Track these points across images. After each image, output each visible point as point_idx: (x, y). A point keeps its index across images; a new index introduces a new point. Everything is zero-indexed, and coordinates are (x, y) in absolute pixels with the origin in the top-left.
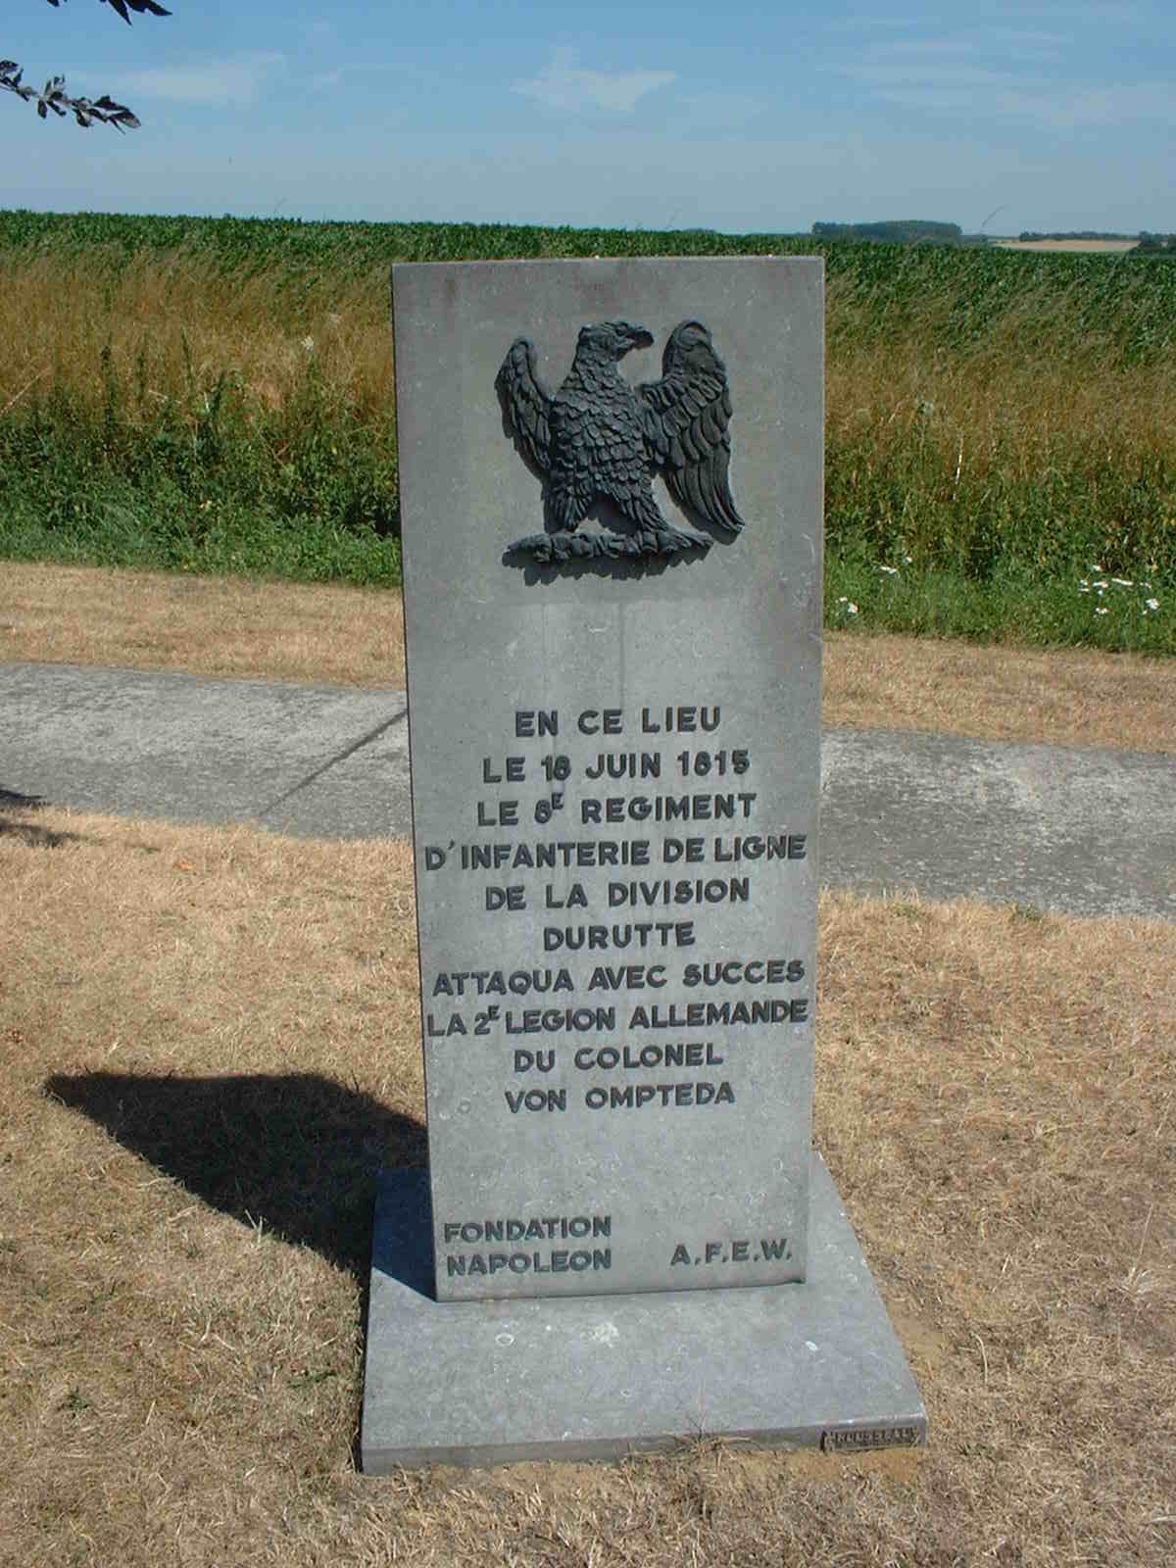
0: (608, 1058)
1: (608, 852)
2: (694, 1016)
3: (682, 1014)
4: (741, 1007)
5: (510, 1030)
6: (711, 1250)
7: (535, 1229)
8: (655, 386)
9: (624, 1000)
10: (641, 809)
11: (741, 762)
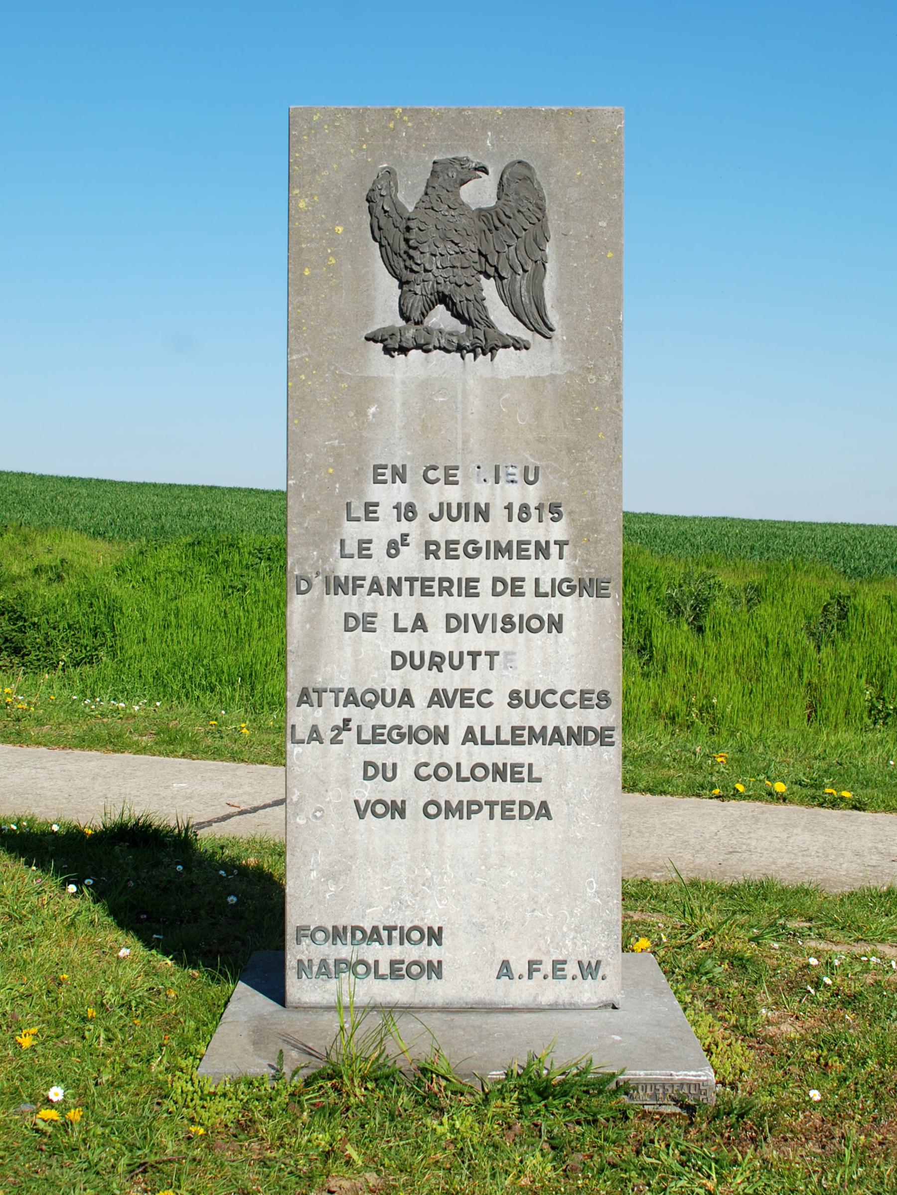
0: (443, 772)
1: (446, 586)
2: (516, 737)
3: (506, 735)
4: (557, 730)
5: (360, 741)
6: (533, 967)
7: (374, 935)
8: (488, 210)
9: (458, 720)
10: (473, 549)
11: (555, 510)
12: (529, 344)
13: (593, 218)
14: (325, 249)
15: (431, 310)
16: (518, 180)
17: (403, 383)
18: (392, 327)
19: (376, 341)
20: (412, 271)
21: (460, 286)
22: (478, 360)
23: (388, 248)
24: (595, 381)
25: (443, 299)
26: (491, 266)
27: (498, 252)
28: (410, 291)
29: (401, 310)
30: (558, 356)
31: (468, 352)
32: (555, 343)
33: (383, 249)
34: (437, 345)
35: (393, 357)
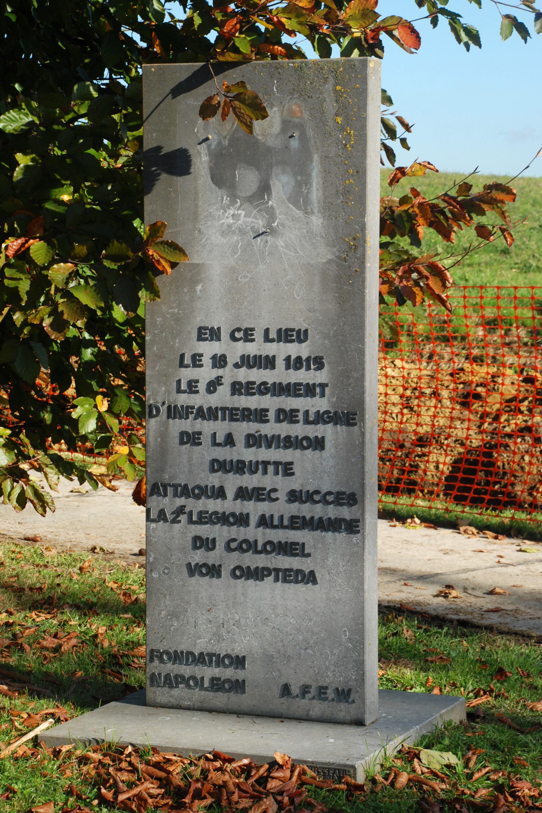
9: (254, 509)
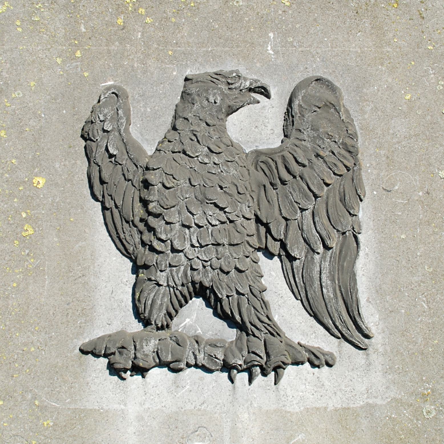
8: (270, 154)
12: (334, 360)
13: (430, 165)
14: (17, 212)
15: (181, 306)
16: (314, 107)
17: (140, 418)
18: (121, 333)
19: (97, 356)
20: (152, 249)
21: (227, 273)
22: (255, 382)
23: (115, 211)
24: (434, 413)
25: (201, 291)
26: (275, 240)
27: (286, 219)
28: (150, 280)
29: (135, 308)
30: (377, 378)
31: (239, 371)
32: (373, 357)
33: (108, 213)
34: (193, 362)
35: (123, 379)
